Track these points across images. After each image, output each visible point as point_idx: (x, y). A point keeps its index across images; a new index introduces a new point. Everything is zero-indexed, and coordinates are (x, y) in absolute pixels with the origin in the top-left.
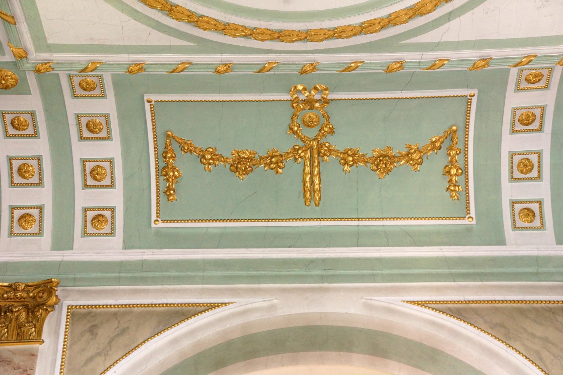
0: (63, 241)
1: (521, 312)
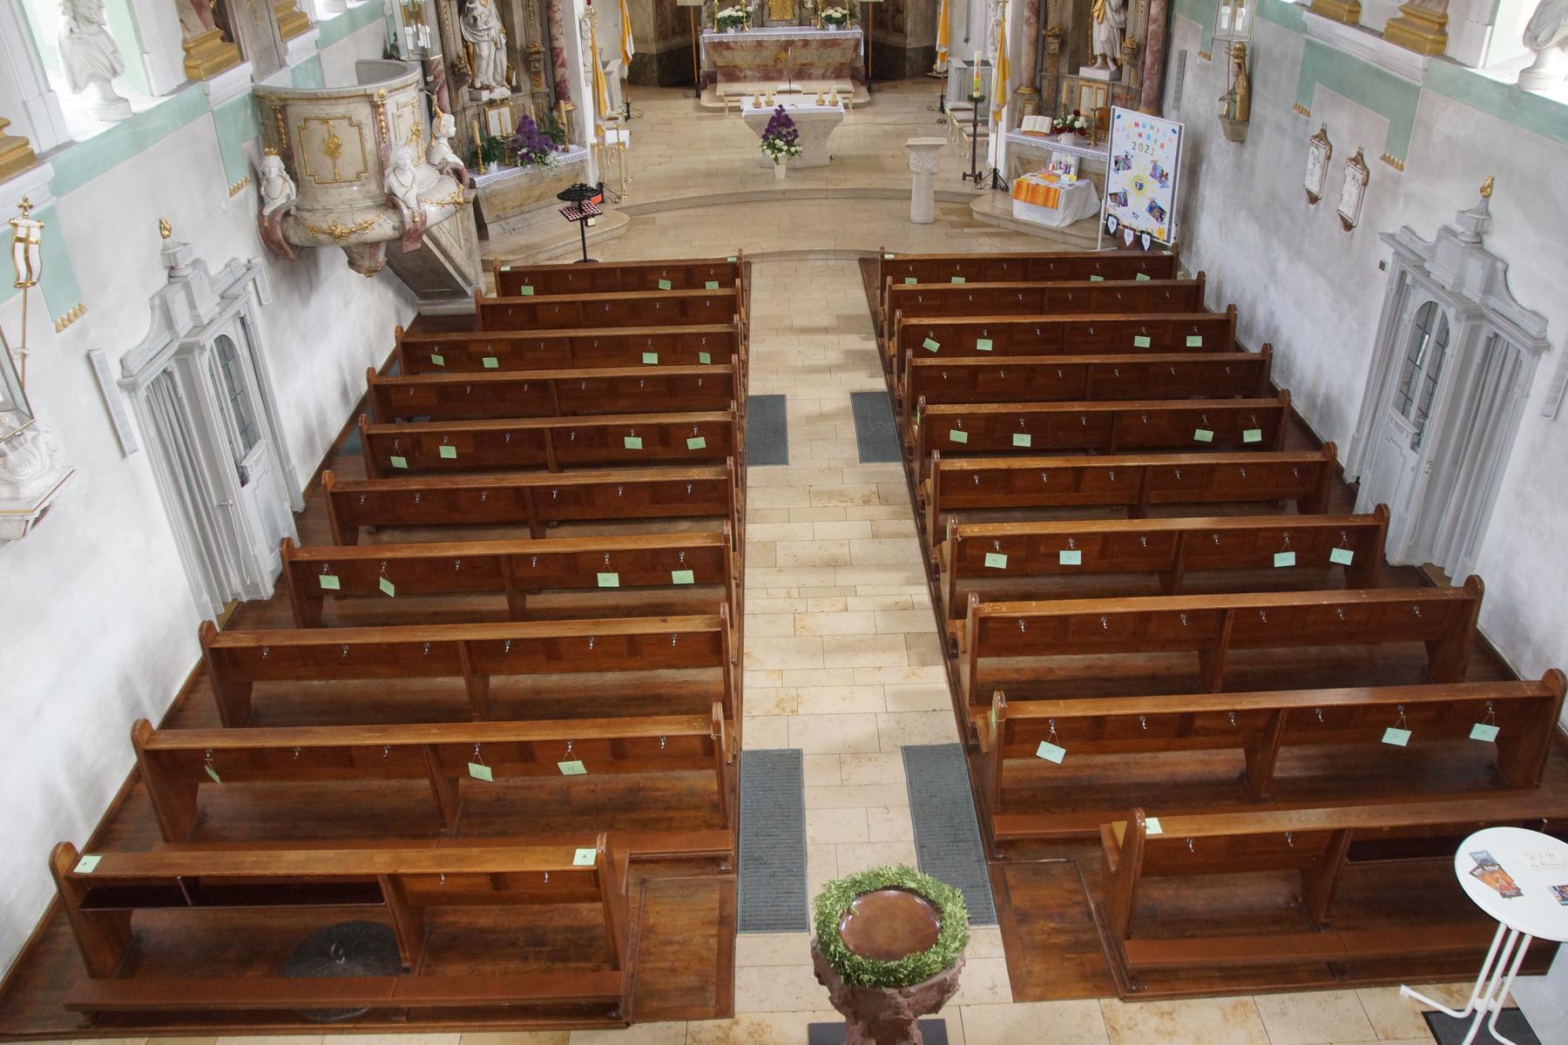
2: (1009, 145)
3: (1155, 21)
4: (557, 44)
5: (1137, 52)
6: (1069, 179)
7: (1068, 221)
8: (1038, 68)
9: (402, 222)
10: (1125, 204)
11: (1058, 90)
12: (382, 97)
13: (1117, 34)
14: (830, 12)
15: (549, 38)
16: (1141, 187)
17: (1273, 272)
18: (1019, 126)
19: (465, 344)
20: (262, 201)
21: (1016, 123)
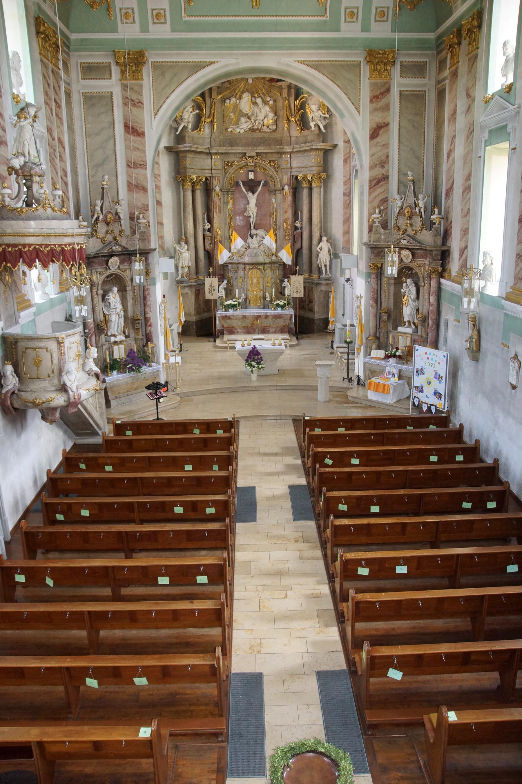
0: (145, 29)
1: (342, 66)
2: (365, 364)
3: (432, 305)
4: (148, 316)
5: (425, 320)
6: (394, 380)
7: (395, 400)
8: (377, 328)
9: (69, 398)
10: (422, 391)
11: (387, 338)
12: (63, 339)
13: (415, 311)
14: (278, 302)
16: (430, 383)
17: (496, 423)
18: (370, 355)
19: (96, 459)
21: (368, 353)
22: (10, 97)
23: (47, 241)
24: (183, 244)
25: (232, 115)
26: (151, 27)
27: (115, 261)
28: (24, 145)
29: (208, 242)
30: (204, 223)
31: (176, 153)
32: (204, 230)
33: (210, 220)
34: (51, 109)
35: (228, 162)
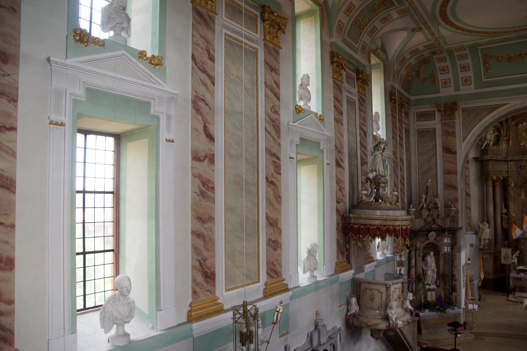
0: (457, 89)
4: (454, 273)
9: (389, 325)
12: (390, 285)
15: (452, 271)
20: (348, 311)
22: (371, 137)
23: (385, 223)
24: (485, 223)
25: (524, 134)
26: (462, 88)
27: (432, 235)
28: (376, 166)
29: (504, 223)
30: (502, 208)
31: (482, 161)
32: (502, 214)
33: (506, 207)
34: (396, 141)
35: (521, 166)
